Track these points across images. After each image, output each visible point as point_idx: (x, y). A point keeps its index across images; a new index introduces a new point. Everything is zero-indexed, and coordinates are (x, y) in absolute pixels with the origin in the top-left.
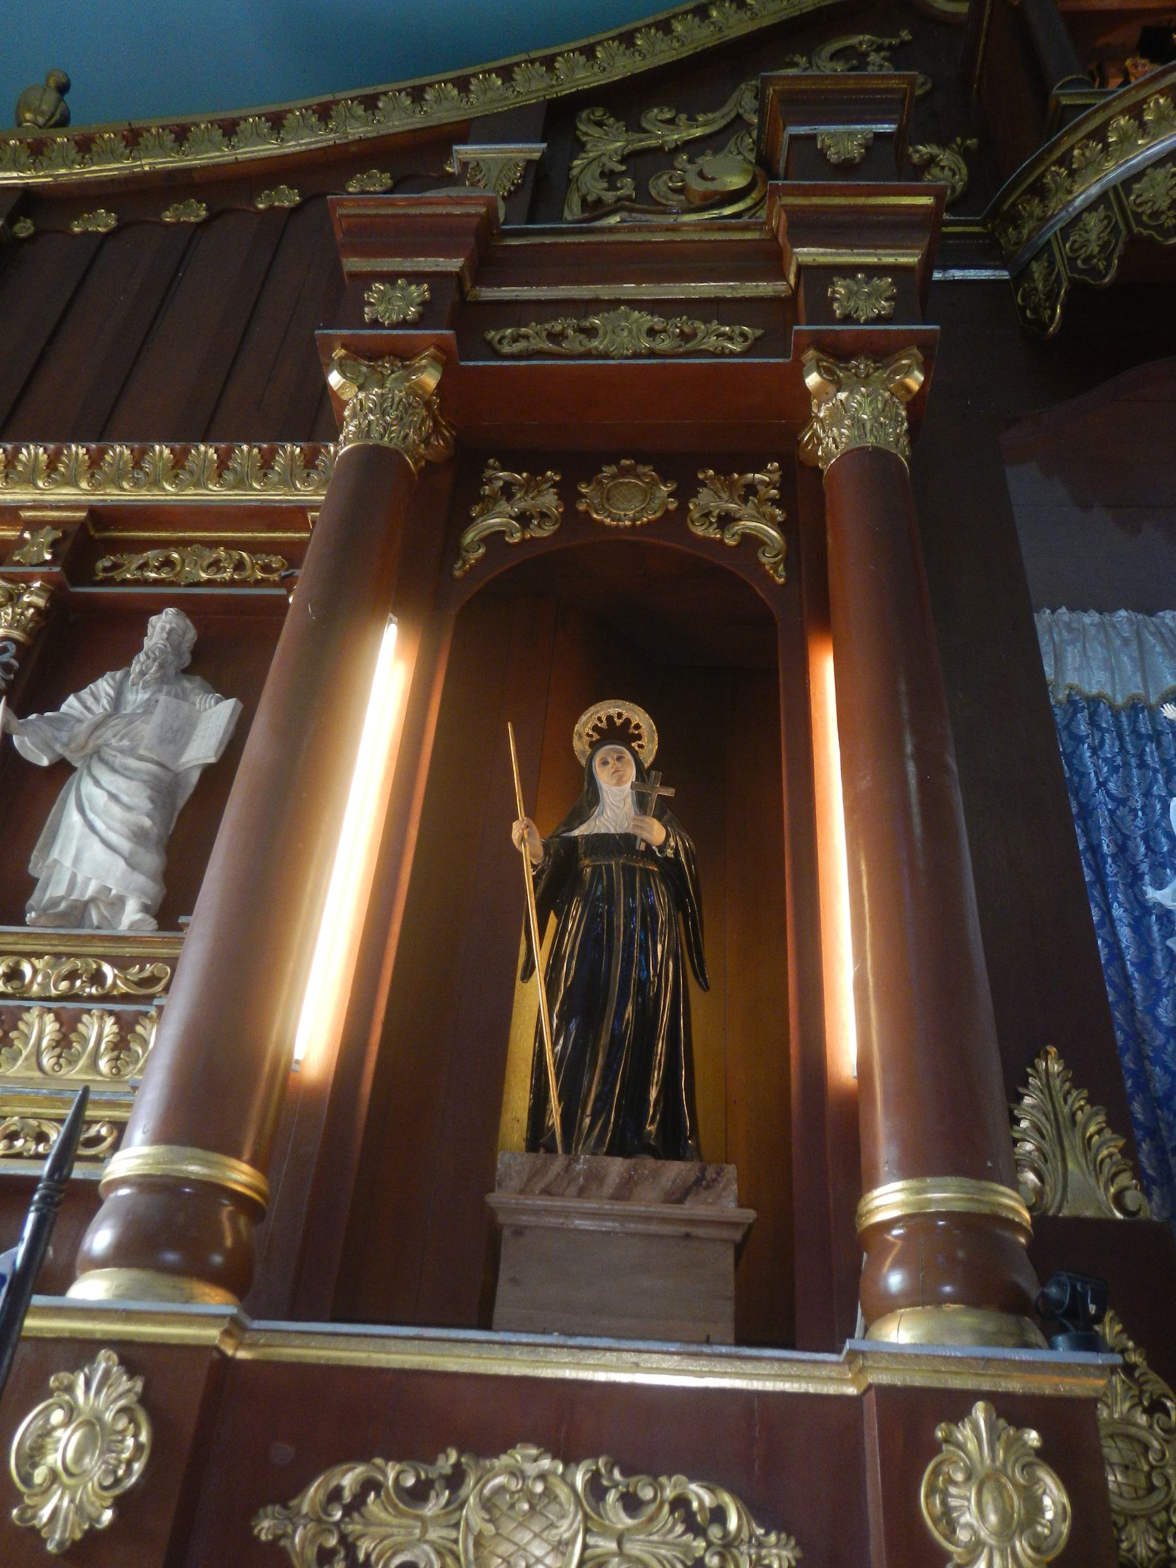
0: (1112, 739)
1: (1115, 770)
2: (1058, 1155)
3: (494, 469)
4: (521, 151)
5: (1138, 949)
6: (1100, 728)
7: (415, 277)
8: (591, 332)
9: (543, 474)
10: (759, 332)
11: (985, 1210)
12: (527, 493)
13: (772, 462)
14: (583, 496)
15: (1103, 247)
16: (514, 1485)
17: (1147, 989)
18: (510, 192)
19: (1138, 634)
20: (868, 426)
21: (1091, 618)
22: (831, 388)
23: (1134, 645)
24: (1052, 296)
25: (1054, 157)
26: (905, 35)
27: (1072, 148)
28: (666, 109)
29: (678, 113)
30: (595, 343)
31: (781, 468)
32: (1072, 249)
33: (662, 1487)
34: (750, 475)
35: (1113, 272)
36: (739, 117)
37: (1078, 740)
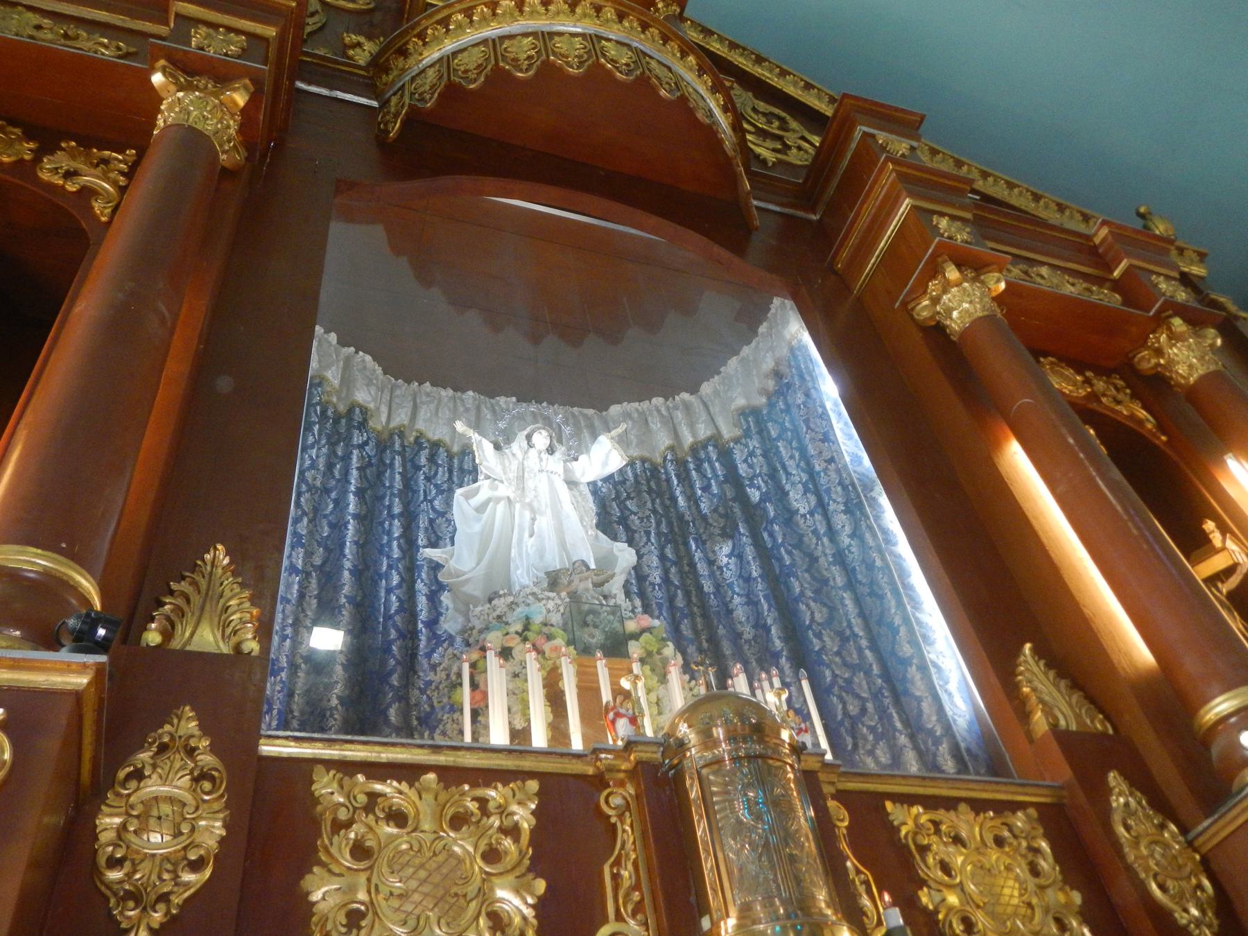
0: (444, 472)
1: (442, 492)
2: (197, 614)
5: (430, 611)
6: (438, 466)
15: (432, 87)
17: (429, 640)
19: (478, 409)
21: (447, 393)
22: (172, 88)
23: (473, 413)
24: (396, 115)
25: (415, 32)
27: (426, 28)
32: (415, 89)
34: (107, 153)
35: (433, 100)
37: (418, 468)
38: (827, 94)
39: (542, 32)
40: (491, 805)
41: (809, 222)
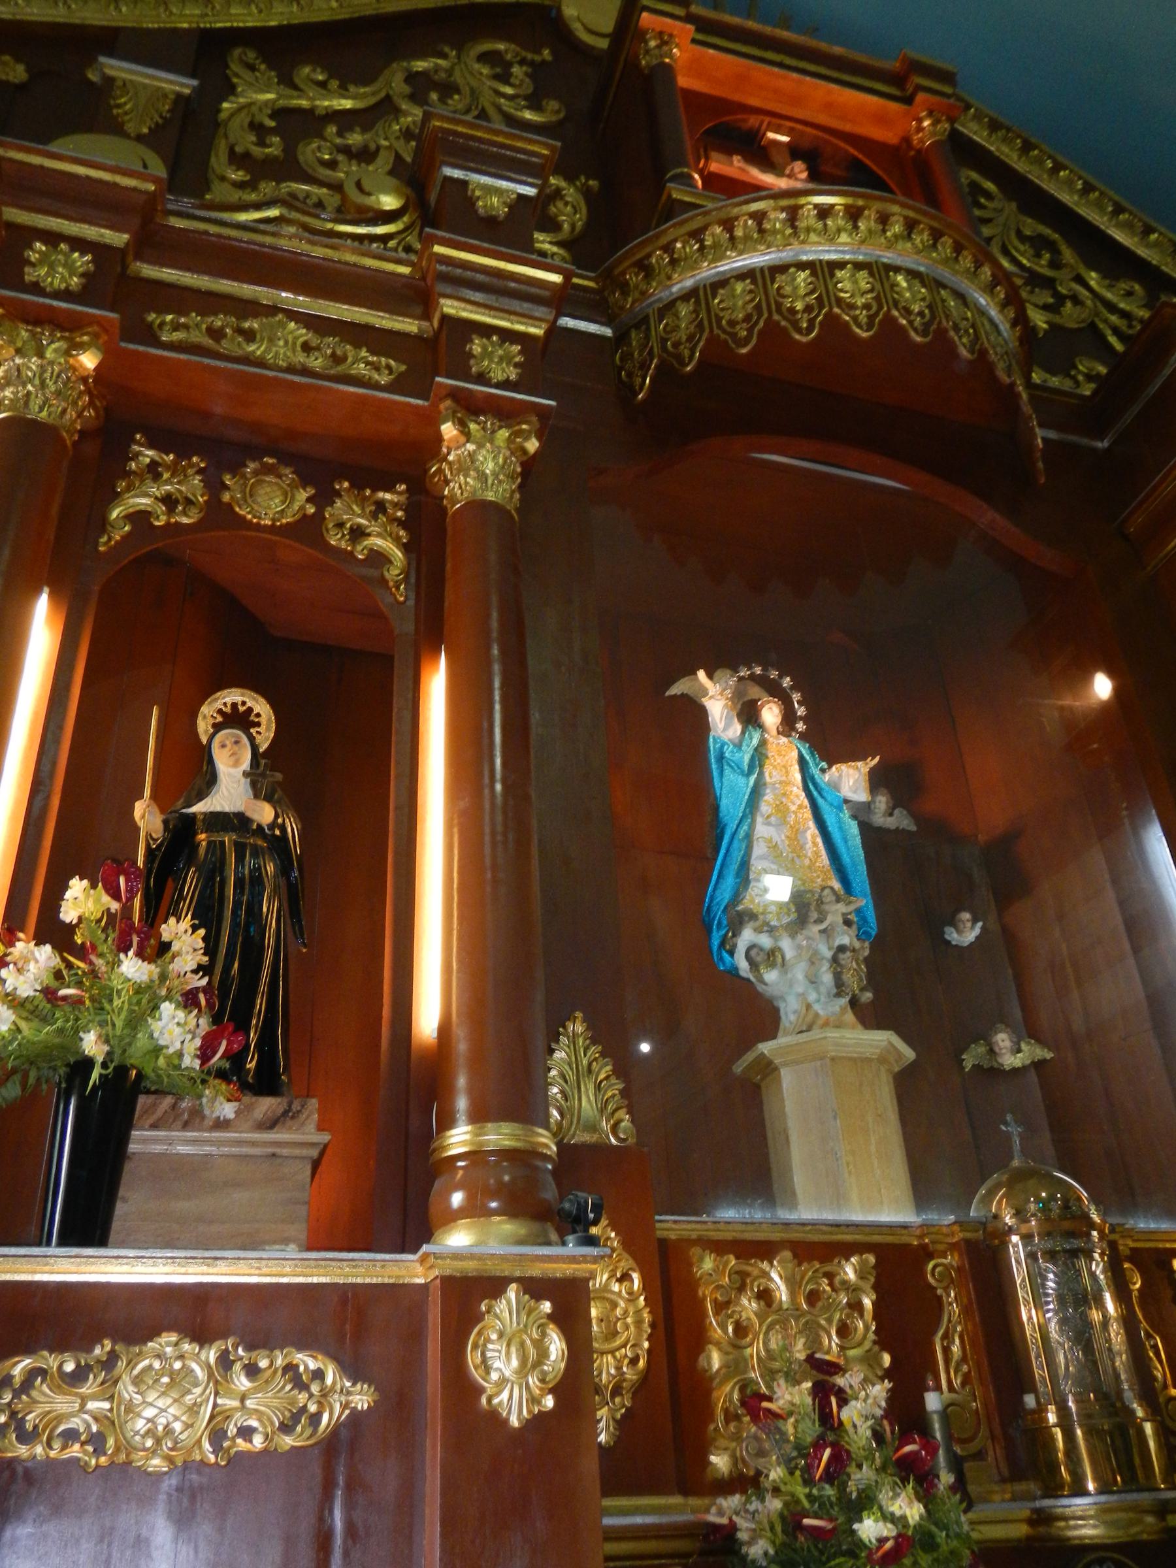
3: (142, 445)
4: (171, 82)
7: (79, 244)
8: (250, 336)
9: (190, 459)
10: (403, 368)
11: (528, 1147)
12: (173, 475)
13: (401, 483)
14: (227, 488)
15: (690, 338)
16: (157, 1365)
18: (157, 124)
20: (490, 482)
22: (463, 439)
24: (644, 367)
26: (546, 53)
27: (676, 240)
28: (319, 70)
29: (331, 77)
30: (252, 348)
31: (408, 490)
33: (276, 1357)
34: (381, 495)
36: (388, 98)
38: (1110, 199)
39: (821, 261)
40: (837, 1280)
41: (1094, 450)
